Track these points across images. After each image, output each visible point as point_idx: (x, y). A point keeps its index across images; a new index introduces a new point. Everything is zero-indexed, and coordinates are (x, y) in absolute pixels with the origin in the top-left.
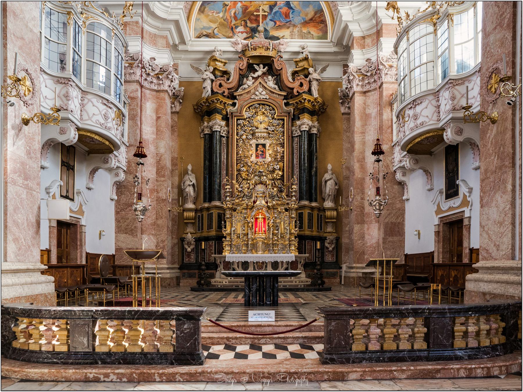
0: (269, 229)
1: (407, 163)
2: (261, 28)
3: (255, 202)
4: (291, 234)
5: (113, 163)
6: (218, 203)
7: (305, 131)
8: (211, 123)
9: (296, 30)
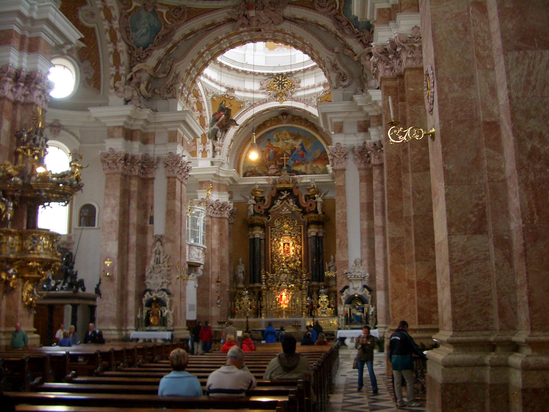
2: (285, 168)
3: (280, 285)
4: (303, 305)
7: (313, 236)
9: (309, 166)
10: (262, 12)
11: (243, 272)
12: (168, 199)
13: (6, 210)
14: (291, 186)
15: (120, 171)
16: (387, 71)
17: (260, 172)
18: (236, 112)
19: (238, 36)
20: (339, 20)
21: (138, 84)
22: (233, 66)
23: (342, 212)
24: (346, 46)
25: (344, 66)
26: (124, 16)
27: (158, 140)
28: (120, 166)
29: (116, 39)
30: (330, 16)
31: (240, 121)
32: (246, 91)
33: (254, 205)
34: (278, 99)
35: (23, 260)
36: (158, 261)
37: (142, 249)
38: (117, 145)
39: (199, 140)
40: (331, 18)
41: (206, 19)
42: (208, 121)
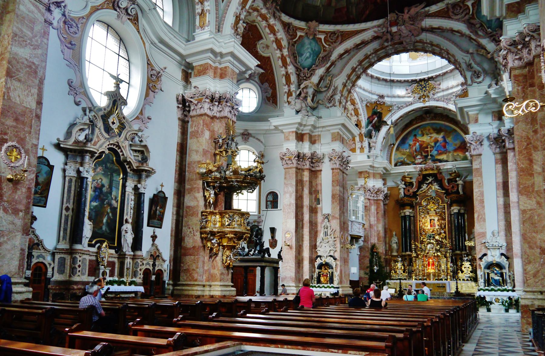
2: (429, 157)
8: (404, 211)
9: (450, 154)
10: (403, 27)
12: (333, 186)
13: (209, 197)
14: (436, 172)
15: (295, 166)
16: (516, 62)
17: (408, 162)
19: (383, 50)
20: (473, 24)
21: (305, 98)
22: (382, 77)
24: (480, 46)
25: (478, 64)
26: (292, 45)
27: (323, 141)
28: (294, 161)
29: (287, 64)
30: (464, 22)
33: (404, 189)
34: (421, 100)
35: (222, 232)
36: (326, 234)
37: (313, 225)
38: (292, 146)
39: (357, 139)
40: (465, 23)
41: (357, 40)
42: (364, 124)
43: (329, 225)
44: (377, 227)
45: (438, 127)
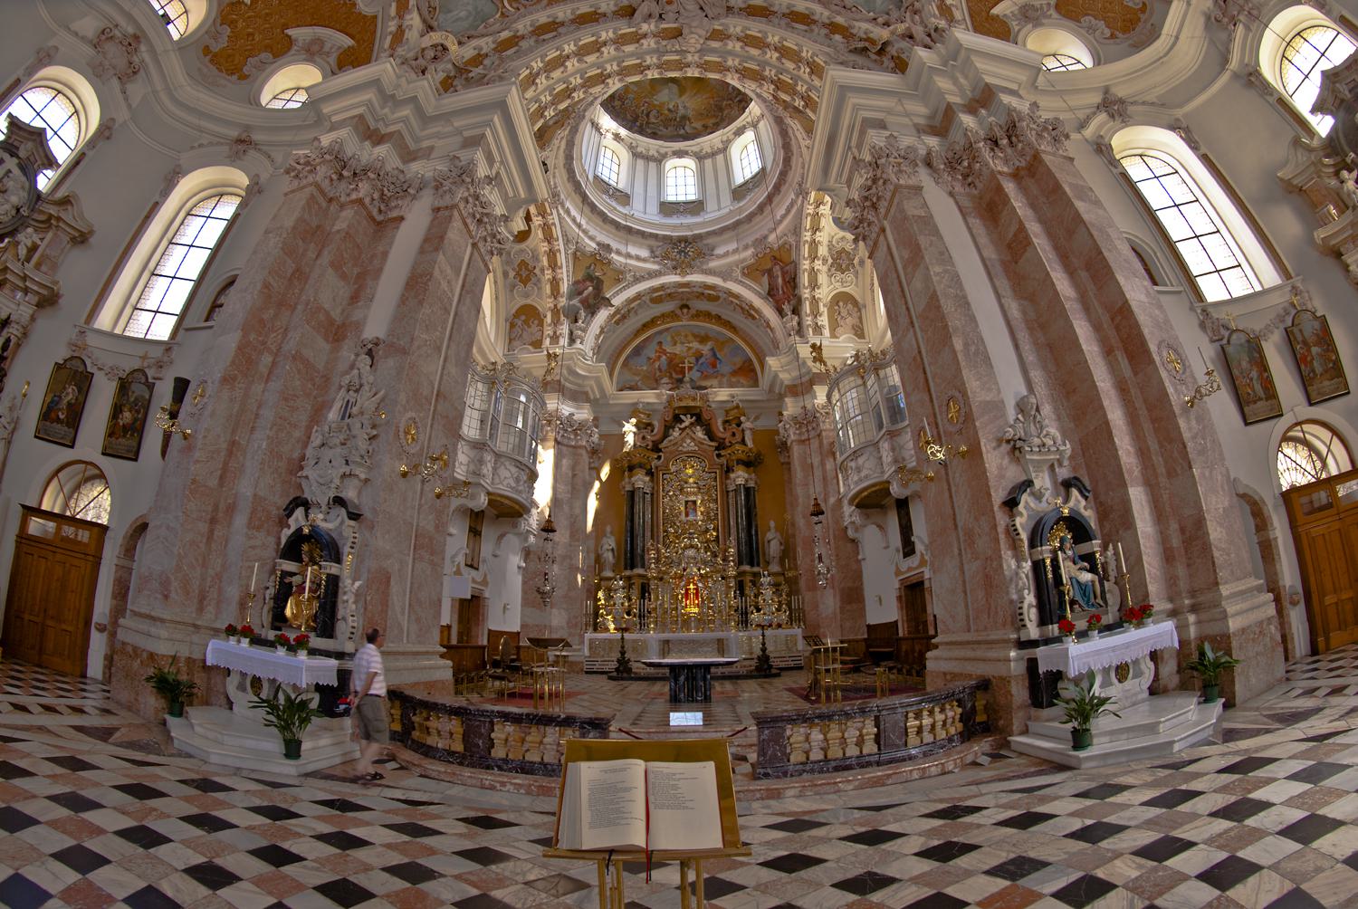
0: (703, 601)
1: (857, 519)
2: (687, 379)
3: (685, 570)
4: (730, 607)
5: (523, 526)
6: (639, 571)
9: (725, 380)
11: (612, 550)
14: (698, 404)
18: (609, 288)
23: (946, 271)
31: (618, 301)
32: (628, 256)
36: (346, 413)
39: (549, 319)
43: (368, 377)
44: (571, 508)
45: (703, 333)
